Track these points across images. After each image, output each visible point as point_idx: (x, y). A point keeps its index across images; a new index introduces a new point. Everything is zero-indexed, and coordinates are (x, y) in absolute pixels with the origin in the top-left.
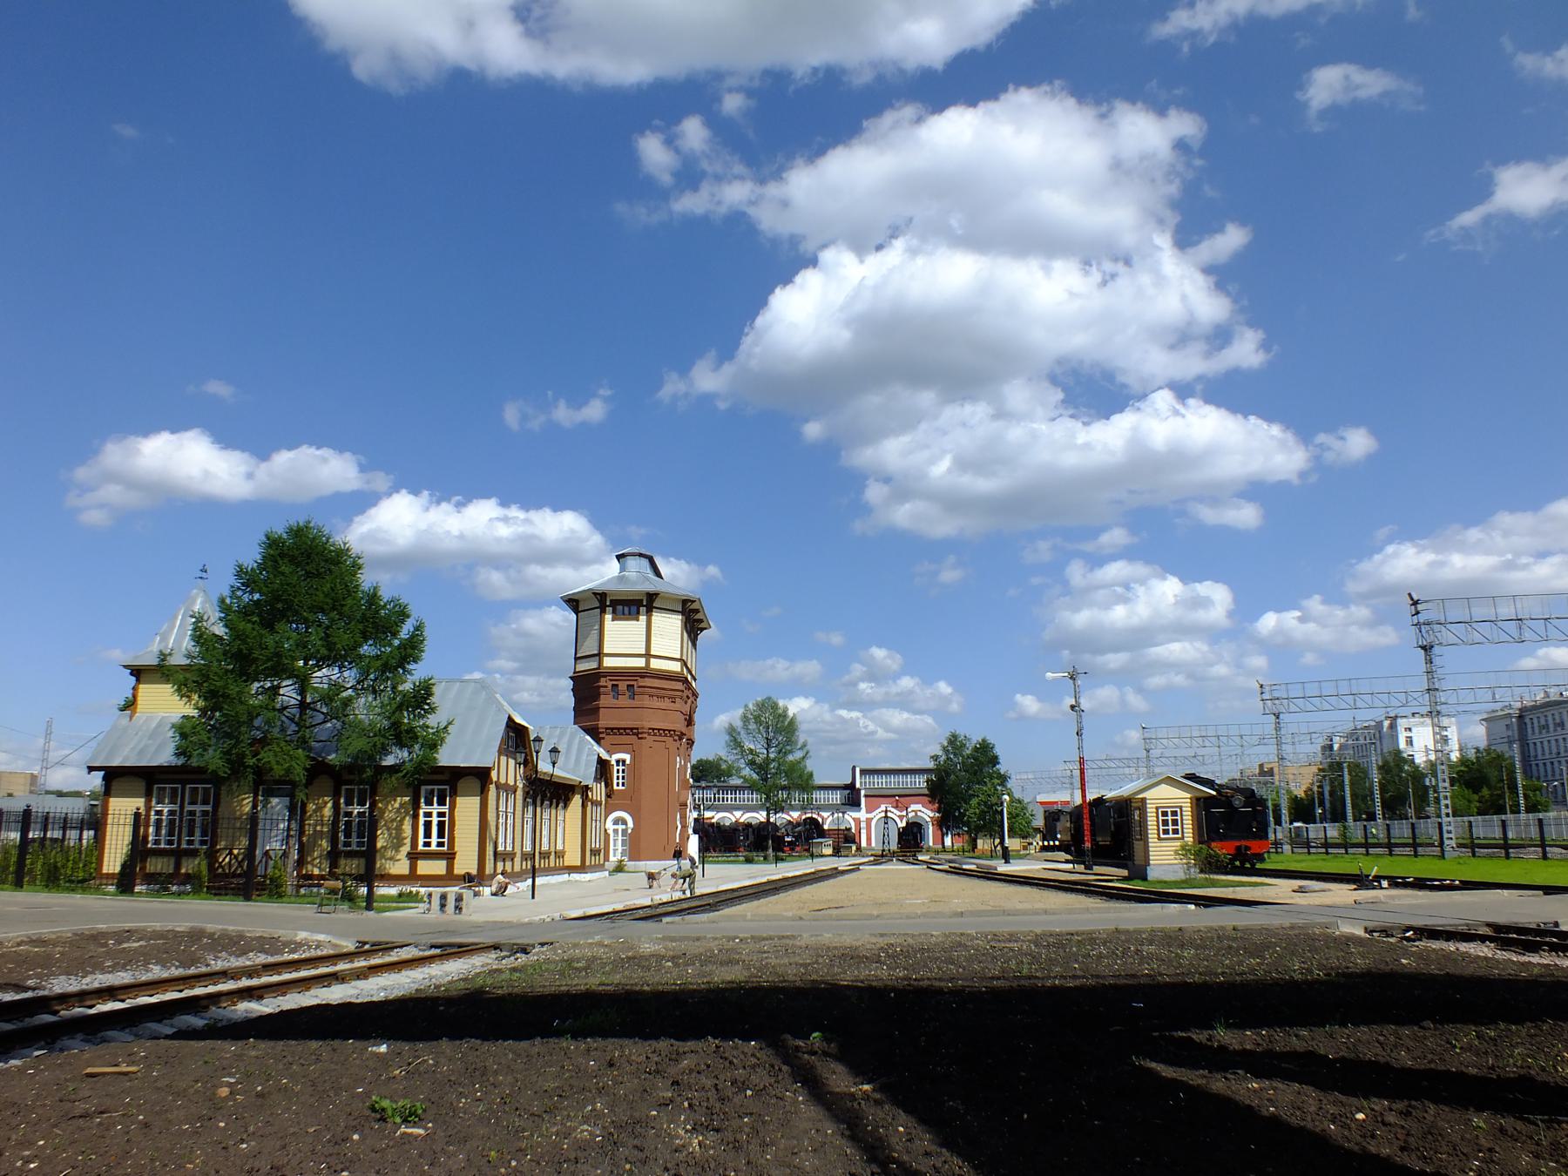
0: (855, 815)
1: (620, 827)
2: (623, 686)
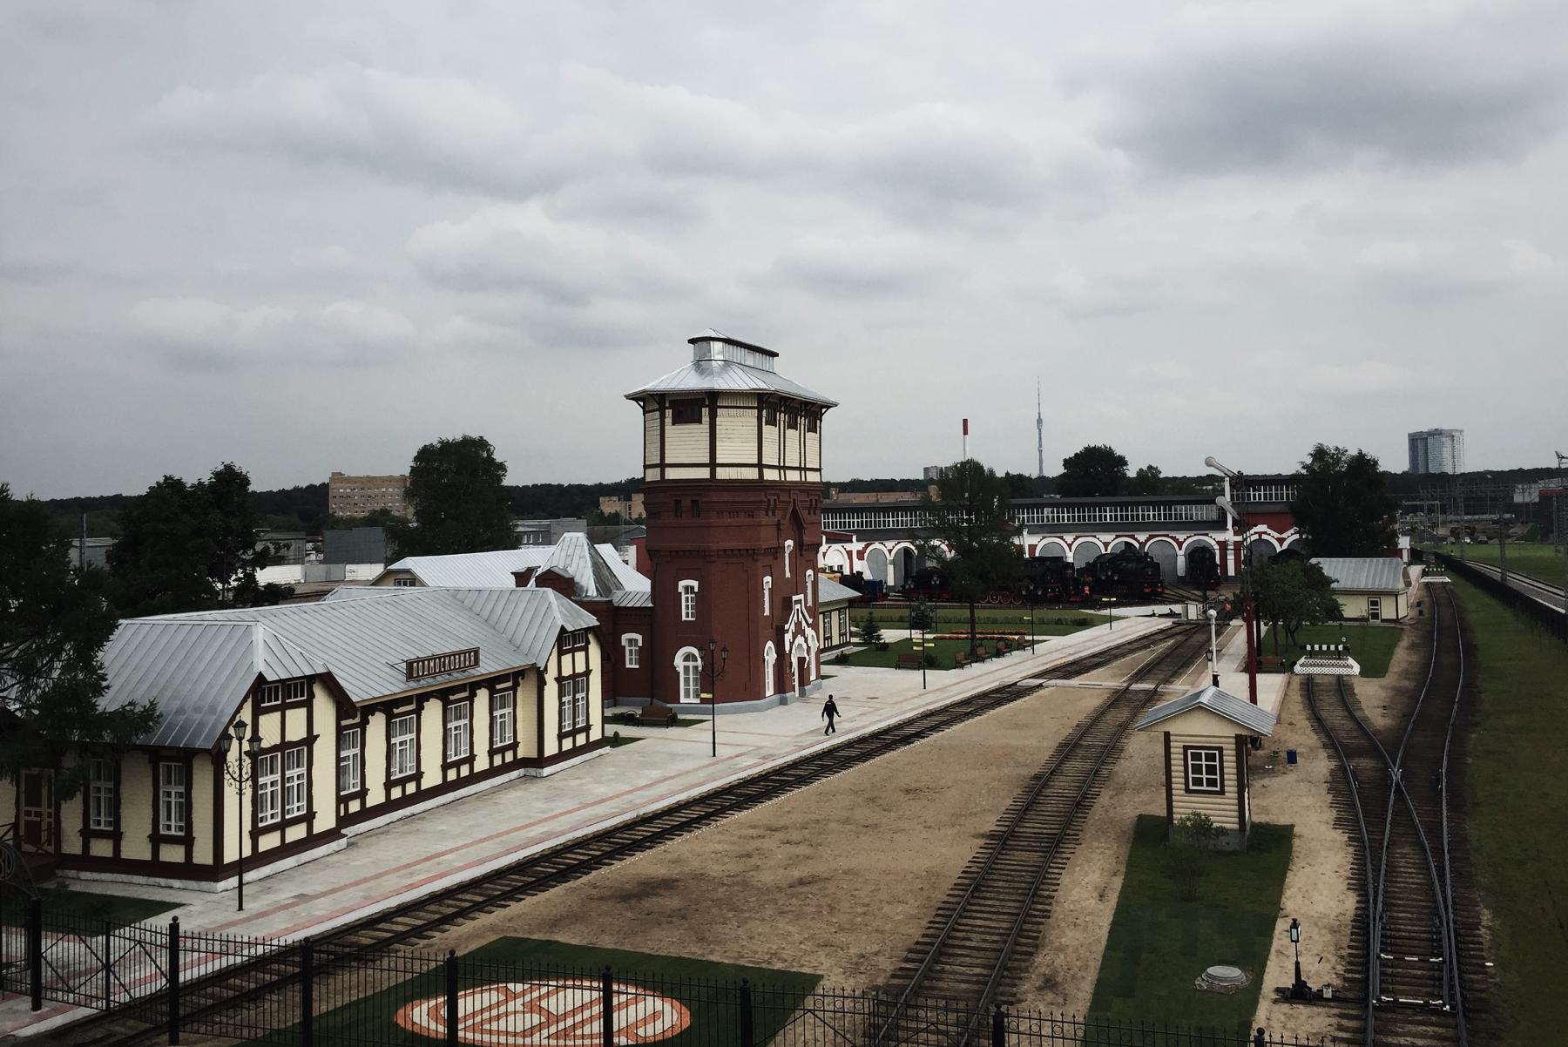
0: (1220, 537)
1: (691, 664)
2: (686, 502)
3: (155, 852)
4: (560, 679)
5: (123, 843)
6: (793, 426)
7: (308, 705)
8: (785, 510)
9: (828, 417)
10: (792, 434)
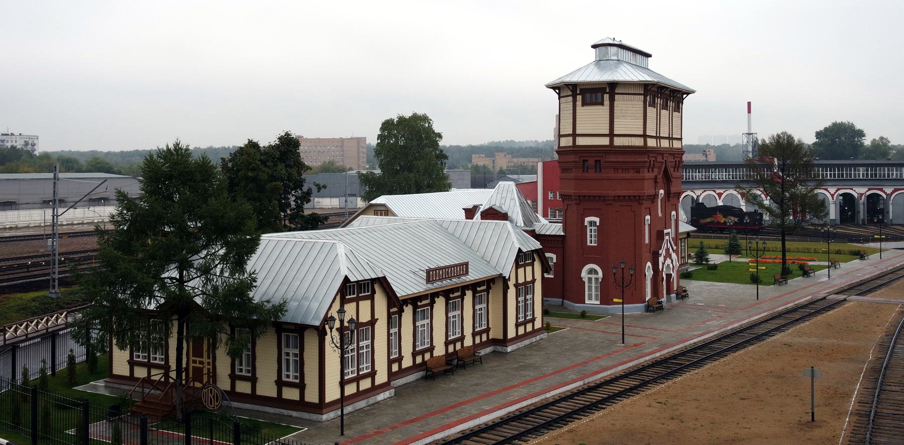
1: (593, 276)
3: (280, 392)
4: (517, 285)
5: (258, 385)
6: (665, 107)
7: (372, 298)
8: (660, 168)
9: (688, 101)
10: (664, 113)
